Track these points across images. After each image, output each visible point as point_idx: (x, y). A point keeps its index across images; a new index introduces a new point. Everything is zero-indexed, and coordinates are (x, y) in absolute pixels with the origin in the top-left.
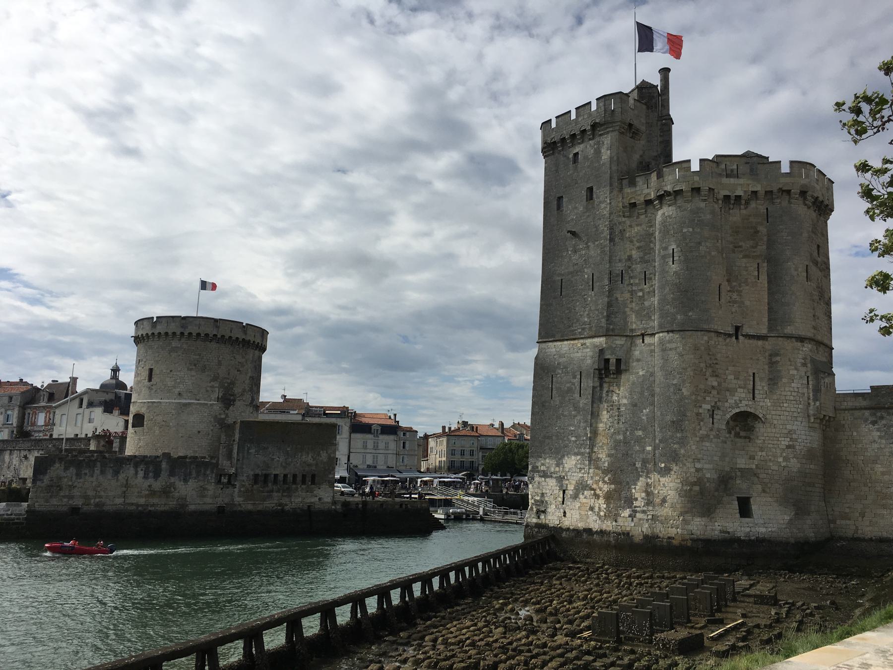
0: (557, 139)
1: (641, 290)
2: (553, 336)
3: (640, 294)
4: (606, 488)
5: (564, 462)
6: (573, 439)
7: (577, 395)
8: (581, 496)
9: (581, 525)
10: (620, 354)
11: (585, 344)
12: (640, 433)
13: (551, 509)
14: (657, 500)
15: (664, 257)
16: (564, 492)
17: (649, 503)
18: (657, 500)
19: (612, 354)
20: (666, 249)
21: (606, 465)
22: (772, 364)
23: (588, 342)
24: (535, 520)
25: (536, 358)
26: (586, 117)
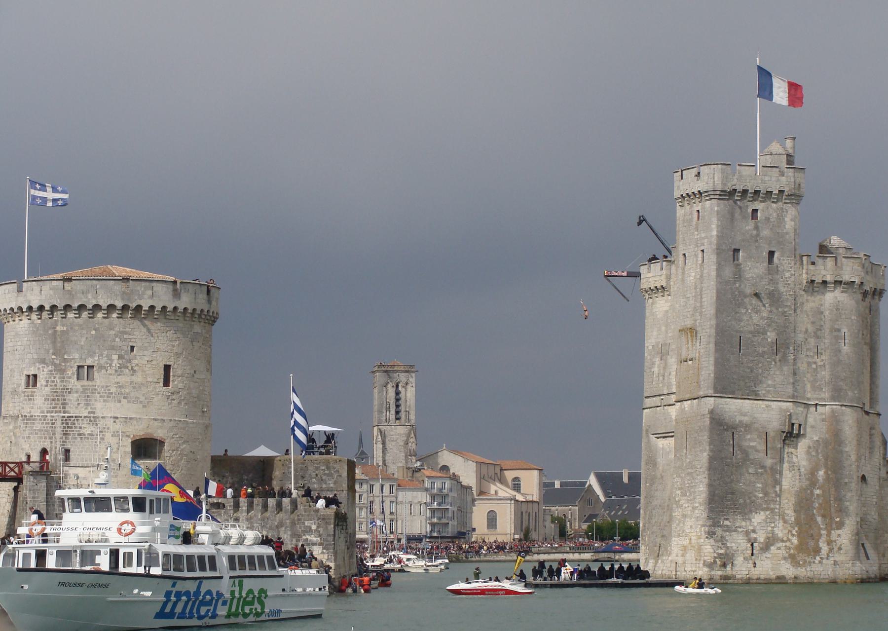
0: (740, 188)
1: (815, 363)
2: (733, 393)
3: (814, 366)
4: (795, 540)
5: (751, 516)
6: (761, 495)
7: (763, 455)
8: (772, 548)
9: (772, 575)
10: (802, 422)
11: (770, 406)
12: (818, 492)
13: (739, 560)
14: (836, 549)
15: (837, 338)
16: (752, 545)
17: (831, 550)
18: (836, 549)
19: (797, 419)
20: (839, 330)
21: (793, 519)
22: (871, 435)
23: (774, 405)
24: (720, 573)
25: (712, 412)
26: (773, 179)
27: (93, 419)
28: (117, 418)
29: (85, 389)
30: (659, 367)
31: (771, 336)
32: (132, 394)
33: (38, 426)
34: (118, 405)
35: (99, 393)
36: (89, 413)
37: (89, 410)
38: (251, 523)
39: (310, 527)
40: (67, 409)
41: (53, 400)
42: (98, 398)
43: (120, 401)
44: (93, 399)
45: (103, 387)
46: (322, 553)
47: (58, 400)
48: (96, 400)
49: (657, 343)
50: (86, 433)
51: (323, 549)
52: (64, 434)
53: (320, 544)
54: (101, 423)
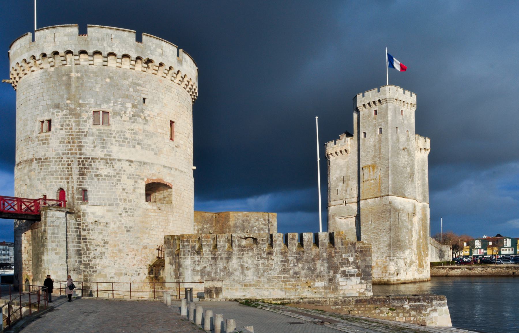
27: (109, 161)
28: (132, 161)
29: (100, 134)
30: (342, 186)
31: (409, 169)
32: (145, 141)
33: (53, 167)
34: (133, 149)
35: (115, 137)
36: (105, 155)
37: (106, 153)
38: (286, 257)
39: (347, 260)
40: (84, 150)
41: (69, 142)
42: (114, 142)
43: (134, 147)
44: (109, 143)
45: (118, 132)
46: (361, 283)
47: (74, 142)
48: (112, 144)
49: (340, 177)
50: (103, 174)
51: (362, 279)
52: (81, 175)
53: (358, 275)
54: (117, 165)
